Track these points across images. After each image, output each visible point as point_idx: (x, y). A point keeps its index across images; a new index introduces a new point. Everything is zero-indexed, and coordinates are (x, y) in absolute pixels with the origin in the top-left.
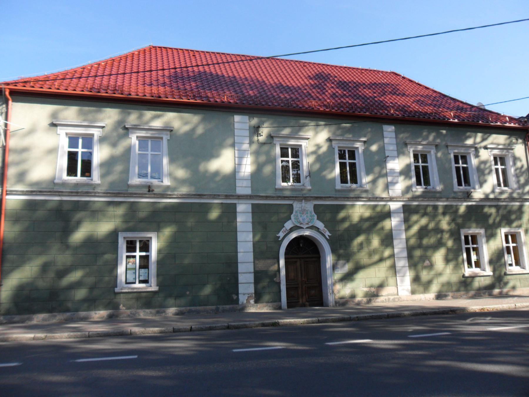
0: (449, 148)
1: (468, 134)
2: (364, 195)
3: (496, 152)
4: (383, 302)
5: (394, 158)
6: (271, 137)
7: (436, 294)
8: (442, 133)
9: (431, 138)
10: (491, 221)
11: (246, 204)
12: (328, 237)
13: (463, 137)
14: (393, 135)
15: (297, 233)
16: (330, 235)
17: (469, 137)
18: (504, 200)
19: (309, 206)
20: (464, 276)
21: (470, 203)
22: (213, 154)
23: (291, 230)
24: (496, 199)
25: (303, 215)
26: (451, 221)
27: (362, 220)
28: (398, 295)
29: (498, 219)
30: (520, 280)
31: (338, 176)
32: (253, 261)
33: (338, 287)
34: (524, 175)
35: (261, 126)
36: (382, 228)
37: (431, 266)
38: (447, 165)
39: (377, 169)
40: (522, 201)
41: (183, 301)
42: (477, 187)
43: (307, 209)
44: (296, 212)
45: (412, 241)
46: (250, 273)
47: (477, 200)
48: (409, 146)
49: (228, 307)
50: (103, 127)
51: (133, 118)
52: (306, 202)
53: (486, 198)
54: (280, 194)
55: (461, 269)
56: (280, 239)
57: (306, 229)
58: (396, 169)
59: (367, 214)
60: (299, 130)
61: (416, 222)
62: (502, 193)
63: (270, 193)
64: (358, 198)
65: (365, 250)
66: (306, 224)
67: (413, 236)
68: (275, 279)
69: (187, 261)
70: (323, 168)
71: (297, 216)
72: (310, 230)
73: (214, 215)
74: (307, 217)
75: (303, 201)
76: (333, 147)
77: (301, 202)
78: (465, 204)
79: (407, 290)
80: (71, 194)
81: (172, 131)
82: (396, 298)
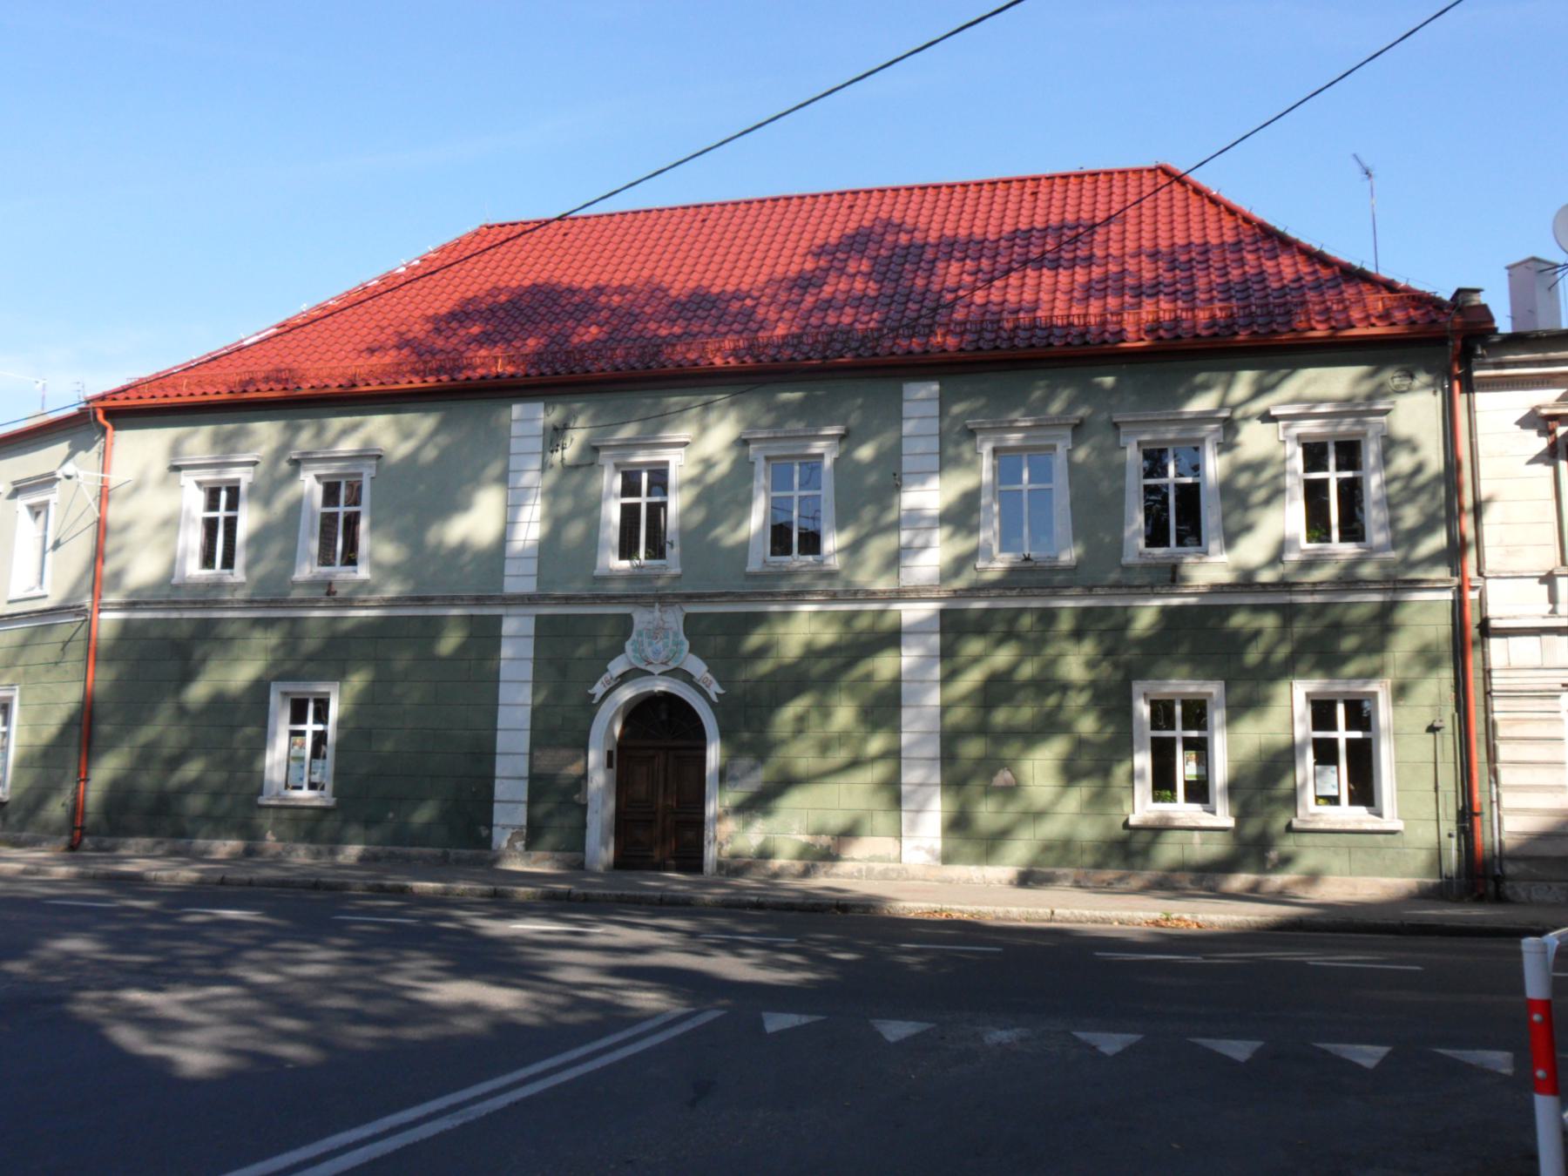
0: (1122, 430)
1: (1201, 378)
2: (822, 585)
3: (1309, 427)
4: (851, 876)
5: (922, 476)
6: (592, 450)
7: (1022, 869)
8: (1099, 385)
9: (1056, 407)
10: (1253, 656)
11: (525, 615)
12: (715, 698)
13: (1181, 390)
14: (934, 408)
15: (633, 689)
16: (721, 691)
17: (1206, 387)
18: (1314, 588)
19: (673, 618)
20: (1126, 825)
21: (1175, 601)
22: (454, 502)
23: (624, 678)
24: (1284, 585)
25: (655, 642)
26: (1099, 657)
27: (812, 653)
28: (901, 862)
29: (1282, 652)
30: (1350, 853)
31: (757, 535)
32: (527, 751)
33: (729, 826)
34: (1423, 499)
35: (571, 425)
36: (868, 677)
37: (1011, 791)
38: (1105, 487)
39: (868, 513)
40: (1395, 590)
41: (376, 833)
42: (1214, 545)
43: (666, 626)
44: (640, 634)
45: (959, 715)
46: (520, 778)
47: (1202, 590)
48: (979, 438)
49: (467, 853)
50: (255, 463)
51: (305, 439)
52: (664, 609)
53: (1246, 581)
54: (602, 590)
55: (1120, 802)
56: (595, 702)
57: (661, 677)
58: (928, 506)
59: (827, 636)
60: (662, 426)
61: (976, 660)
62: (1309, 564)
63: (576, 588)
64: (798, 595)
65: (814, 733)
66: (662, 663)
67: (964, 698)
68: (576, 797)
69: (388, 746)
70: (710, 522)
71: (642, 644)
72: (670, 679)
73: (449, 643)
74: (665, 646)
75: (657, 605)
76: (751, 460)
77: (651, 609)
78: (1158, 602)
79: (931, 852)
80: (195, 604)
81: (379, 457)
82: (893, 870)
